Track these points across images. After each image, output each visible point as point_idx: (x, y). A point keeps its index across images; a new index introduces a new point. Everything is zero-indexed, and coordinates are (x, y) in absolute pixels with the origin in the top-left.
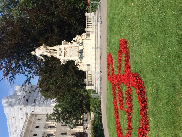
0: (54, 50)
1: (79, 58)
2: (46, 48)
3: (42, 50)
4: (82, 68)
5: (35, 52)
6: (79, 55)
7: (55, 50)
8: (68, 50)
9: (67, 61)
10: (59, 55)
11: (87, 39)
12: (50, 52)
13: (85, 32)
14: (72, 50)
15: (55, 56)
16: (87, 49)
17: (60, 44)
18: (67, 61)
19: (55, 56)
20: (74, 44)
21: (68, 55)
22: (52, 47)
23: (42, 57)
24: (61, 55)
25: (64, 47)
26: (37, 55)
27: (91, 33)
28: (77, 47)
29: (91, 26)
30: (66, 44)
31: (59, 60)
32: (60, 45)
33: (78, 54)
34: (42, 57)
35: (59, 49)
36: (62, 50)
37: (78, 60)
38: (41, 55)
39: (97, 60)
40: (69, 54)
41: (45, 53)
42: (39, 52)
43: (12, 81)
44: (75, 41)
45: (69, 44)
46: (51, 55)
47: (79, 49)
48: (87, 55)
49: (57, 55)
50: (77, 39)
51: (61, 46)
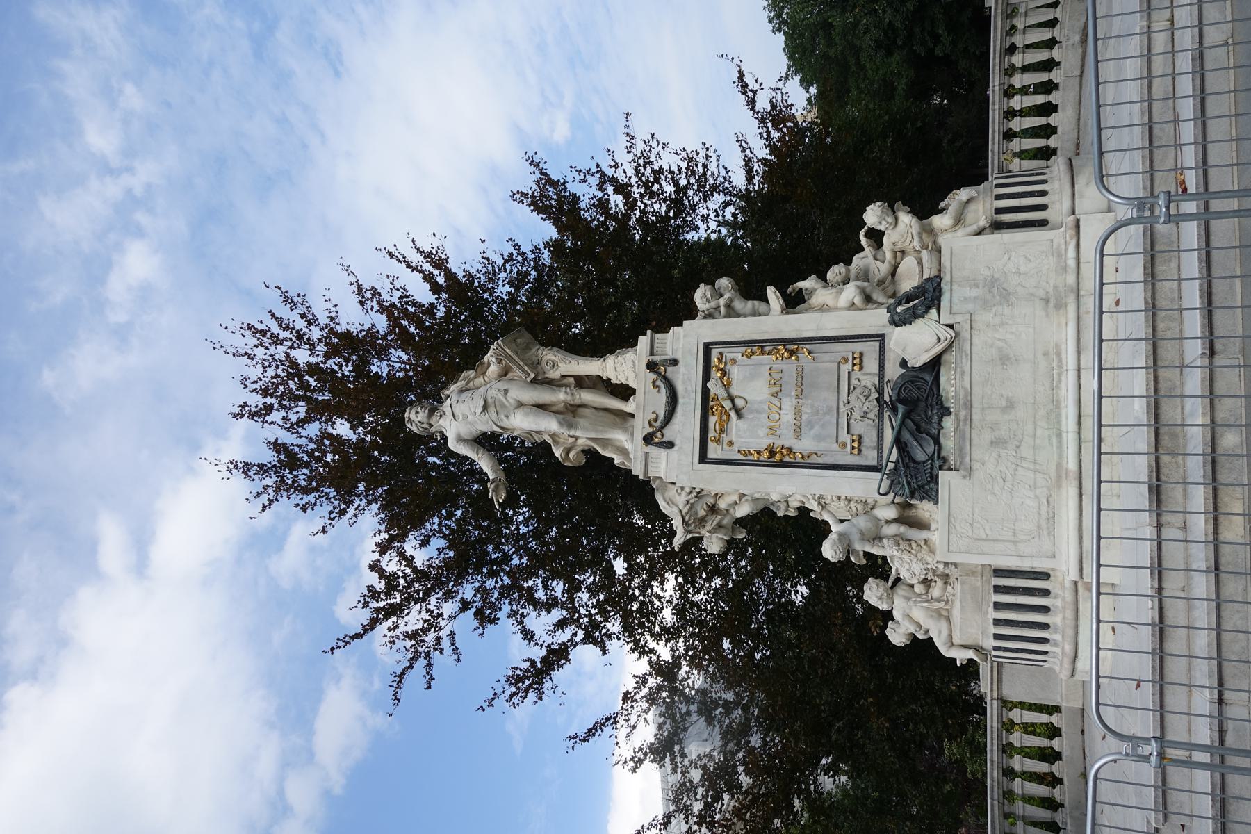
1: (866, 486)
2: (536, 365)
4: (927, 623)
6: (889, 436)
7: (625, 392)
8: (750, 381)
9: (740, 522)
10: (648, 439)
12: (570, 412)
14: (800, 374)
15: (618, 461)
16: (1004, 359)
18: (743, 511)
19: (624, 452)
21: (747, 434)
23: (485, 463)
24: (669, 433)
25: (708, 348)
26: (452, 445)
28: (858, 347)
30: (731, 312)
31: (641, 492)
32: (663, 328)
33: (870, 439)
34: (485, 463)
35: (651, 366)
36: (687, 378)
37: (868, 508)
41: (522, 423)
42: (457, 412)
43: (422, 662)
46: (584, 436)
48: (996, 443)
49: (627, 449)
51: (683, 341)
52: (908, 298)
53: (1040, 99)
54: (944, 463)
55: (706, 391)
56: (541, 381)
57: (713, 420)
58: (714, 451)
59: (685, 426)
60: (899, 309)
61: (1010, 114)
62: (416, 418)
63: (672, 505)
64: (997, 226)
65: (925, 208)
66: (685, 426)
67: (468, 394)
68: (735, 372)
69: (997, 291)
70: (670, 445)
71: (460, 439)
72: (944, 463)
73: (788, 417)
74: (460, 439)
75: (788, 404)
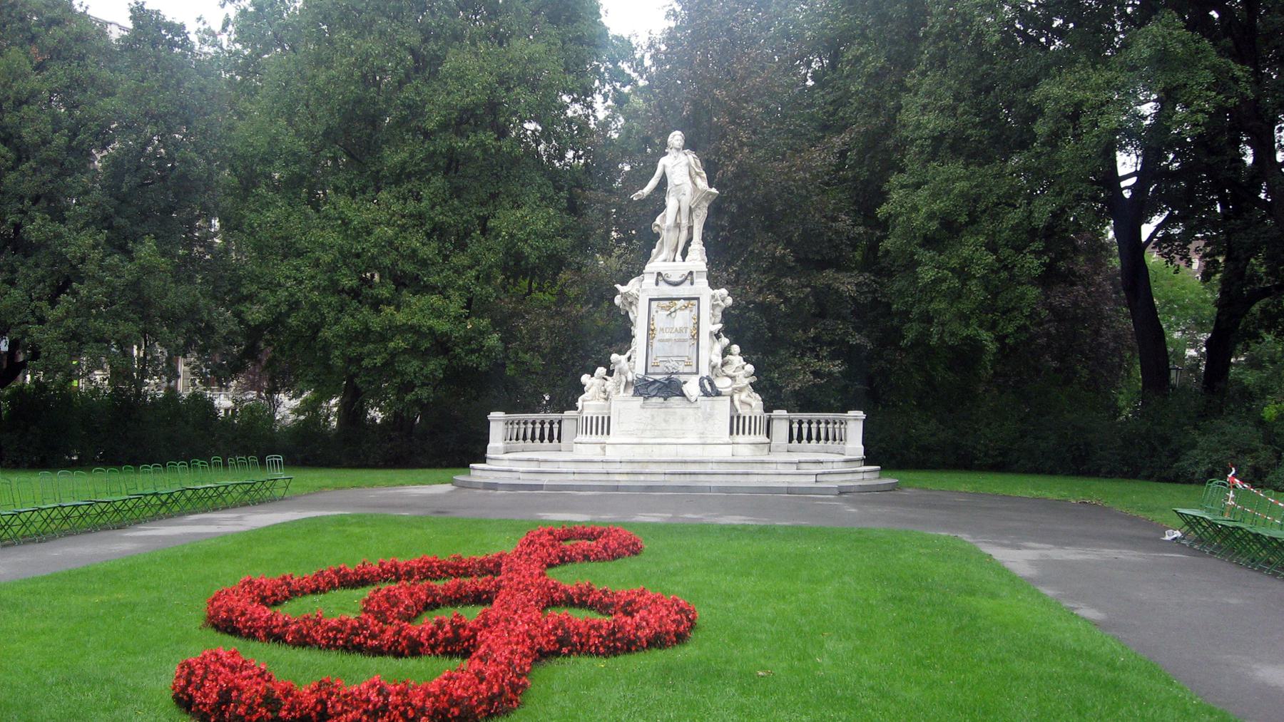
0: (688, 243)
3: (688, 187)
5: (678, 150)
6: (657, 377)
10: (659, 274)
11: (732, 418)
13: (768, 409)
14: (685, 341)
15: (654, 251)
17: (714, 284)
20: (711, 351)
21: (660, 318)
22: (703, 239)
23: (653, 183)
25: (698, 299)
26: (663, 161)
27: (762, 438)
29: (795, 441)
30: (714, 307)
33: (658, 370)
34: (653, 183)
35: (691, 273)
36: (685, 290)
38: (663, 182)
39: (628, 468)
40: (661, 325)
42: (677, 168)
44: (723, 356)
45: (710, 324)
47: (682, 378)
50: (734, 368)
52: (711, 384)
53: (823, 435)
54: (646, 399)
55: (679, 299)
56: (691, 211)
57: (667, 303)
58: (654, 304)
59: (666, 291)
60: (706, 382)
61: (819, 422)
62: (676, 138)
63: (632, 286)
64: (738, 417)
65: (756, 387)
66: (666, 291)
67: (686, 170)
68: (687, 312)
69: (709, 417)
70: (657, 284)
71: (664, 167)
72: (646, 399)
73: (667, 336)
74: (664, 167)
75: (673, 336)
